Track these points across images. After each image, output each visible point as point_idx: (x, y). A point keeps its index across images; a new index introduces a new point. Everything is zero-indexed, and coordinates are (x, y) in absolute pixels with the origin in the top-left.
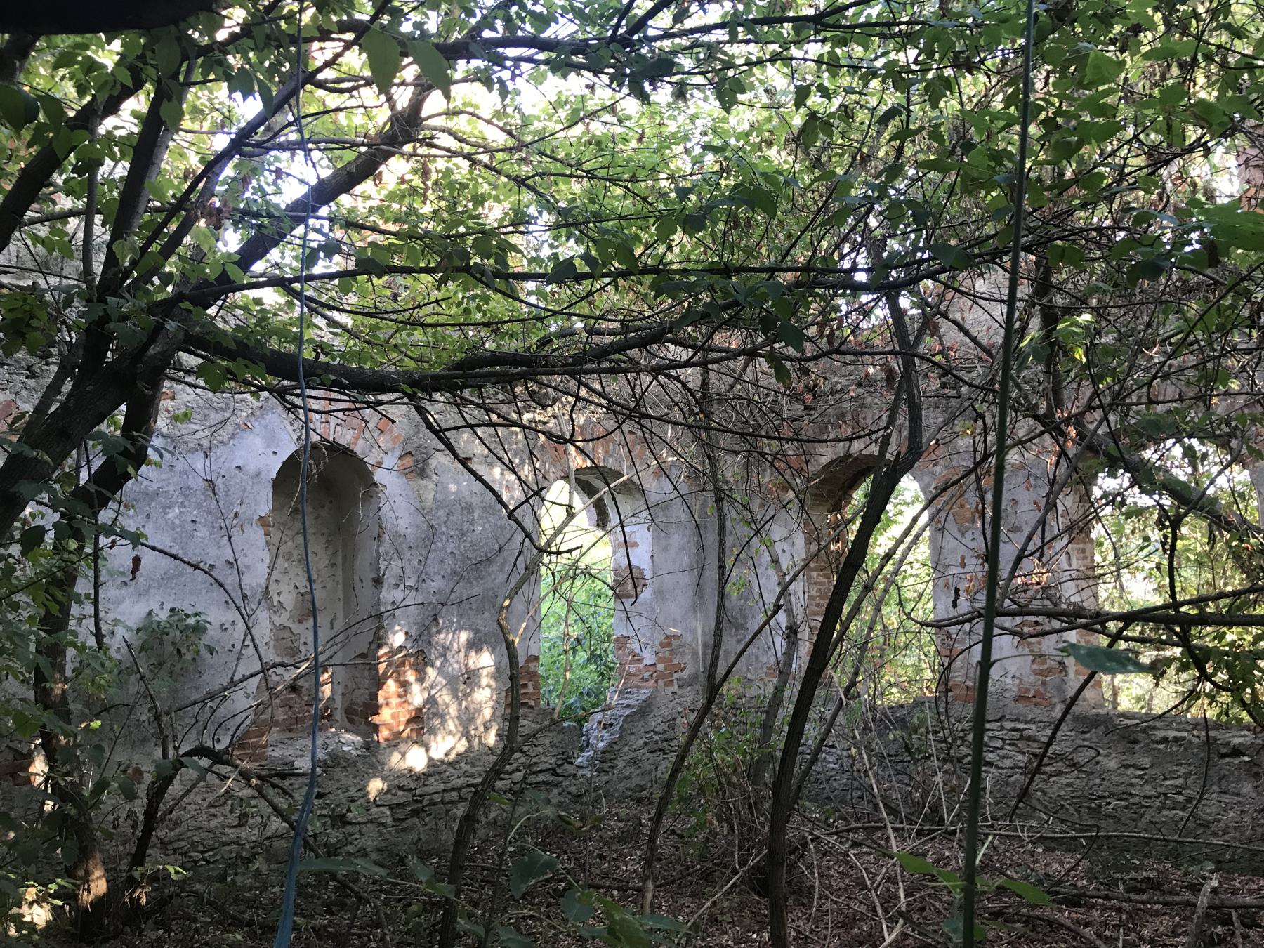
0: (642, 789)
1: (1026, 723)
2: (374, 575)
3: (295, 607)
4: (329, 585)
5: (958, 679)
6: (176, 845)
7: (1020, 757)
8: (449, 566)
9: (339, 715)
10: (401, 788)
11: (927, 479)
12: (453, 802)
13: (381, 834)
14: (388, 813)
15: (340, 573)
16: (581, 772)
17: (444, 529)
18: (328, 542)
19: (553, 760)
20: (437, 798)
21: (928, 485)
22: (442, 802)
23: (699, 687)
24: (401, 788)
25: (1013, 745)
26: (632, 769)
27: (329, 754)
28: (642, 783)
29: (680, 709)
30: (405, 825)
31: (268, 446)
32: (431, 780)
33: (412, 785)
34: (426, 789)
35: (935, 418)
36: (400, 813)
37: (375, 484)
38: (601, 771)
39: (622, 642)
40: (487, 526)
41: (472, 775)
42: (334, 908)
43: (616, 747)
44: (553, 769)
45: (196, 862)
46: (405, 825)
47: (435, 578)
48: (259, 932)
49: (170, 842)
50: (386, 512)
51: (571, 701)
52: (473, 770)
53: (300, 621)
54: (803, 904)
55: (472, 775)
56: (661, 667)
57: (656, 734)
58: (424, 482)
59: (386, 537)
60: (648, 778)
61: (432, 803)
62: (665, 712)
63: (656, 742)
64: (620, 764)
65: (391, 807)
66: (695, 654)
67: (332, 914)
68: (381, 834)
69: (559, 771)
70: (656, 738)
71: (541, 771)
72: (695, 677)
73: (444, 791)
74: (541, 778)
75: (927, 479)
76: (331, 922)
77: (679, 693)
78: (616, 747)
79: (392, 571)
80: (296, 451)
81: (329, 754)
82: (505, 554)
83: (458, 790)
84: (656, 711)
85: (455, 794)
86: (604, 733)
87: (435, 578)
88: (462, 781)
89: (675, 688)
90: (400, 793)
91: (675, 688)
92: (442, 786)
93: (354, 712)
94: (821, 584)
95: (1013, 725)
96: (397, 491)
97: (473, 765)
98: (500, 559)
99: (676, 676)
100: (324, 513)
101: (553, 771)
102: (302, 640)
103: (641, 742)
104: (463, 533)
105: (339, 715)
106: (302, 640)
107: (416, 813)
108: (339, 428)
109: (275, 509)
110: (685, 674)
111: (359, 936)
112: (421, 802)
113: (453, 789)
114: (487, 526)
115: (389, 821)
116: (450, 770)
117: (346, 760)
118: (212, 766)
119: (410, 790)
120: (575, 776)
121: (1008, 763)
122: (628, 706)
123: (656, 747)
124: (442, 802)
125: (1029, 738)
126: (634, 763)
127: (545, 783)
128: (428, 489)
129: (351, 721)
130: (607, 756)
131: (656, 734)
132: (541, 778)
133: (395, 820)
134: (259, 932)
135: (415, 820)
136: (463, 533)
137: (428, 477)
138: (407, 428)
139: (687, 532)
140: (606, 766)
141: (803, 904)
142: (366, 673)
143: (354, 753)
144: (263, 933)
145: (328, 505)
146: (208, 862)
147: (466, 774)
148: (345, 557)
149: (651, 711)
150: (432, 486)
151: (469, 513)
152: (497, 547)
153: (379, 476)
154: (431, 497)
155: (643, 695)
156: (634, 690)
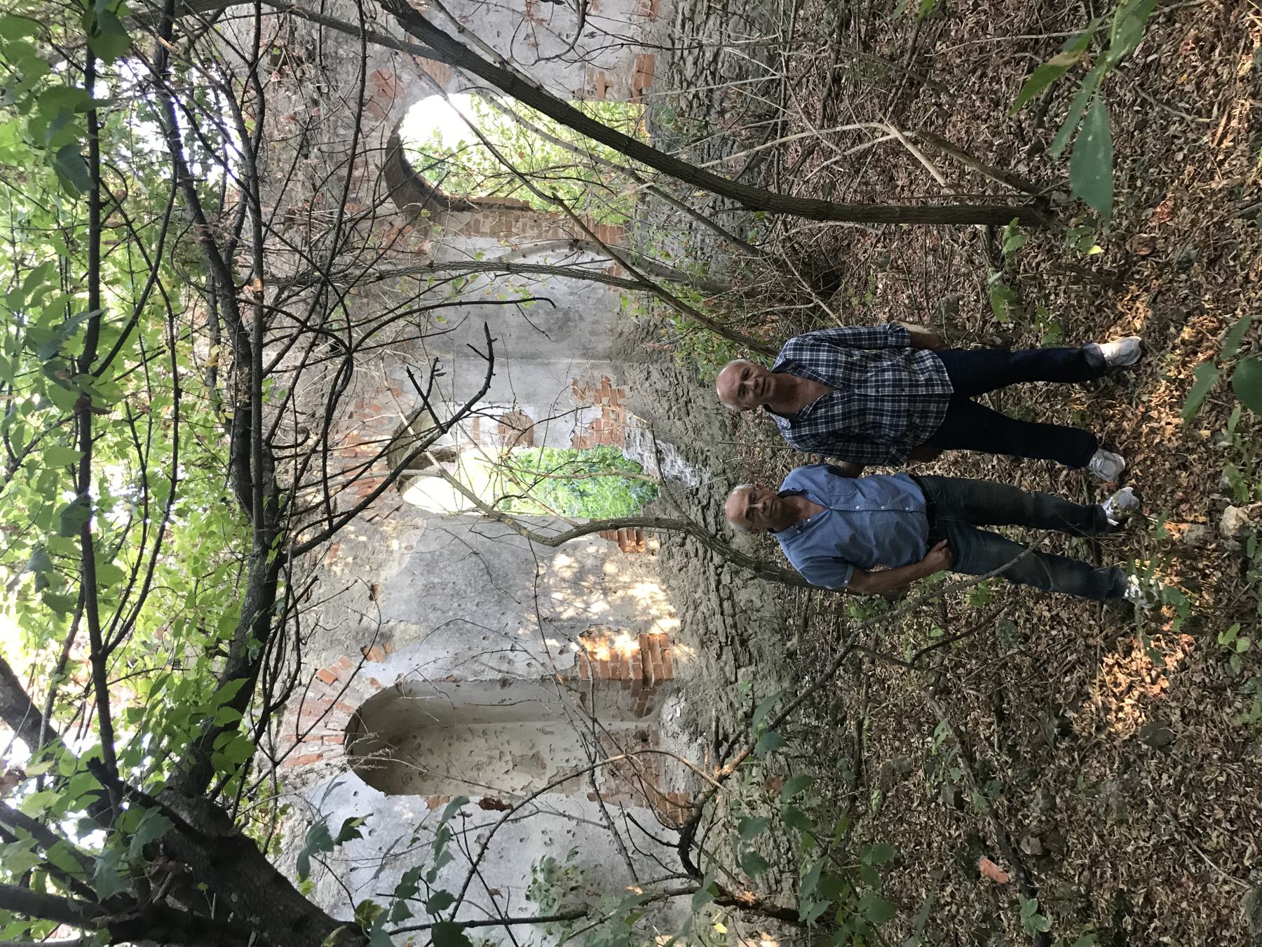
0: (723, 424)
1: (677, 12)
2: (498, 686)
3: (528, 773)
4: (506, 737)
5: (630, 81)
6: (772, 881)
7: (711, 22)
8: (491, 608)
9: (643, 725)
10: (719, 657)
11: (416, 91)
12: (733, 606)
13: (764, 676)
14: (743, 669)
15: (493, 726)
16: (706, 481)
17: (451, 614)
18: (459, 738)
19: (694, 508)
20: (729, 621)
21: (422, 89)
22: (733, 616)
23: (626, 365)
24: (719, 657)
25: (698, 29)
26: (705, 433)
27: (683, 730)
28: (718, 424)
29: (647, 384)
30: (755, 654)
31: (347, 801)
32: (711, 627)
33: (717, 646)
34: (720, 632)
35: (347, 73)
36: (744, 658)
37: (397, 686)
38: (705, 463)
39: (578, 442)
40: (449, 569)
41: (707, 586)
42: (840, 716)
43: (683, 447)
44: (703, 508)
45: (789, 861)
46: (755, 654)
47: (504, 622)
48: (861, 789)
49: (770, 887)
50: (430, 672)
51: (634, 496)
52: (702, 586)
53: (544, 767)
54: (849, 245)
55: (707, 586)
56: (605, 400)
57: (670, 408)
58: (397, 634)
59: (456, 673)
60: (713, 419)
61: (735, 626)
62: (650, 399)
63: (679, 409)
64: (698, 445)
65: (738, 667)
66: (593, 367)
67: (844, 718)
68: (764, 676)
69: (705, 503)
70: (674, 409)
71: (704, 519)
72: (616, 369)
73: (722, 614)
74: (711, 520)
75: (416, 91)
76: (852, 717)
77: (631, 384)
78: (683, 447)
79: (490, 669)
80: (355, 771)
81: (683, 730)
82: (481, 550)
83: (721, 601)
84: (649, 407)
85: (726, 604)
86: (668, 461)
87: (504, 622)
88: (713, 596)
89: (626, 388)
90: (724, 657)
91: (626, 388)
92: (718, 616)
93: (641, 706)
94: (525, 225)
95: (678, 26)
96: (405, 662)
97: (698, 585)
98: (488, 556)
99: (614, 387)
100: (426, 744)
101: (705, 508)
102: (565, 764)
103: (679, 423)
104: (457, 594)
105: (643, 725)
106: (565, 764)
107: (744, 642)
108: (330, 726)
109: (421, 793)
110: (613, 378)
111: (869, 686)
112: (733, 638)
113: (721, 605)
114: (449, 569)
115: (752, 668)
116: (702, 608)
117: (690, 712)
118: (697, 846)
119: (721, 648)
120: (710, 488)
121: (716, 37)
122: (642, 435)
123: (683, 409)
124: (733, 616)
125: (693, 11)
126: (699, 430)
127: (716, 516)
128: (404, 630)
129: (649, 711)
130: (691, 455)
131: (670, 408)
132: (711, 520)
133: (750, 663)
134: (861, 789)
135: (751, 643)
136: (457, 594)
137: (391, 630)
138: (332, 652)
139: (465, 366)
140: (701, 458)
141: (849, 245)
142: (602, 694)
143: (683, 704)
144: (862, 785)
145: (418, 740)
146: (789, 849)
147: (707, 592)
148: (475, 720)
149: (648, 412)
150: (402, 626)
151: (434, 587)
152: (474, 558)
153: (387, 681)
154: (414, 627)
155: (632, 419)
156: (627, 429)
